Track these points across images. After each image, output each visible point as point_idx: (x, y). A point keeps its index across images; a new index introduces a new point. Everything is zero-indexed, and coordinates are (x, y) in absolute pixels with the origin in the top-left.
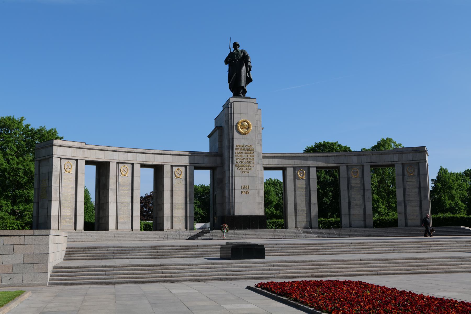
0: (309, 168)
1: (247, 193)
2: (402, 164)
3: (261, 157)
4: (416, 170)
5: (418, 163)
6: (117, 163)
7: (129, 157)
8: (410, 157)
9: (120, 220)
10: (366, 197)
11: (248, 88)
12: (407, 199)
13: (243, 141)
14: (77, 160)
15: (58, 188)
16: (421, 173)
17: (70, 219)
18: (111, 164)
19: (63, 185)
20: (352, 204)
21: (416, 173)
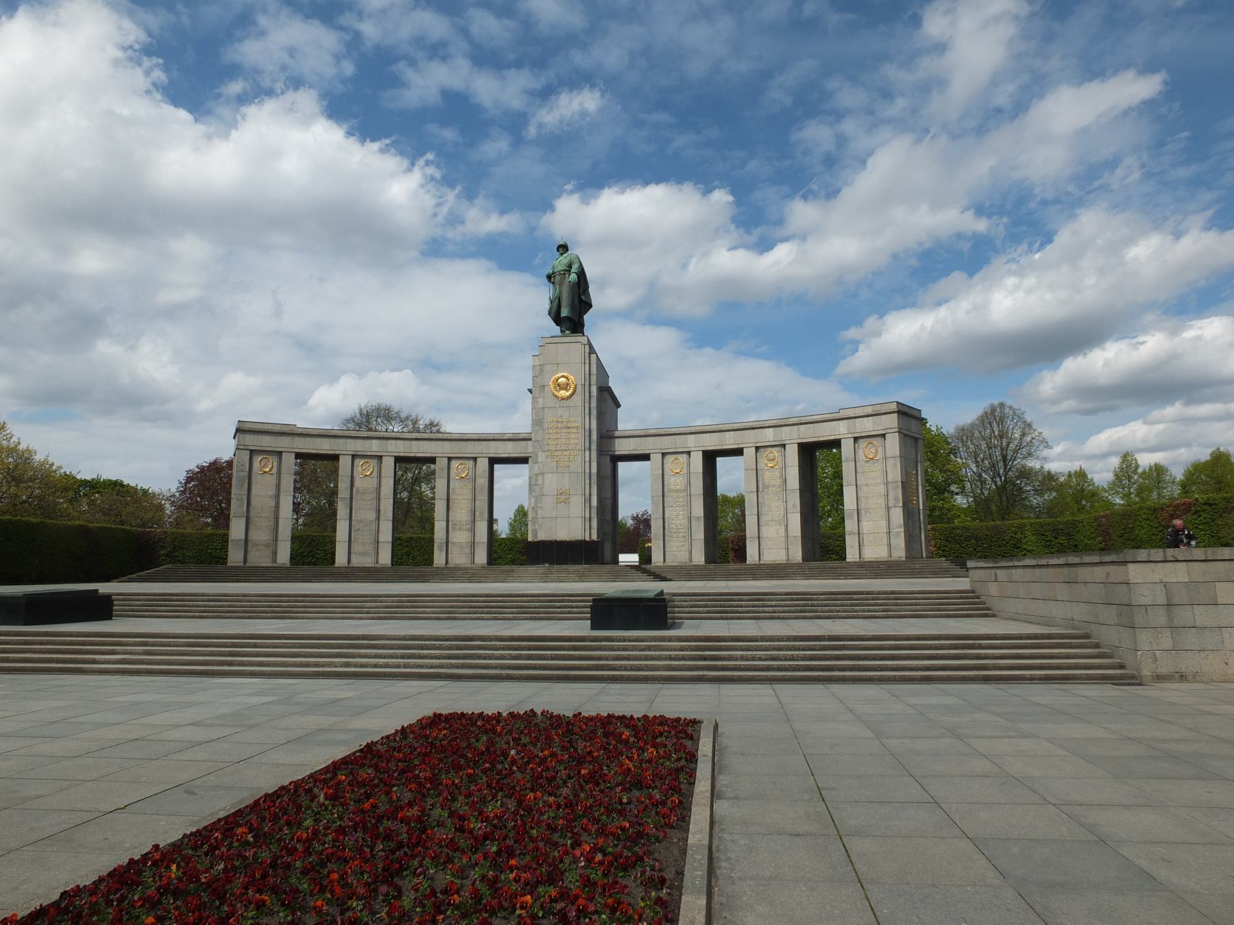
0: (689, 453)
1: (567, 502)
2: (856, 439)
3: (594, 437)
4: (880, 449)
5: (883, 436)
6: (354, 457)
7: (374, 447)
8: (868, 426)
9: (355, 547)
10: (790, 505)
11: (587, 318)
12: (862, 506)
13: (560, 411)
14: (281, 453)
15: (245, 497)
16: (888, 454)
17: (267, 546)
18: (341, 458)
19: (253, 492)
20: (763, 519)
21: (880, 456)
